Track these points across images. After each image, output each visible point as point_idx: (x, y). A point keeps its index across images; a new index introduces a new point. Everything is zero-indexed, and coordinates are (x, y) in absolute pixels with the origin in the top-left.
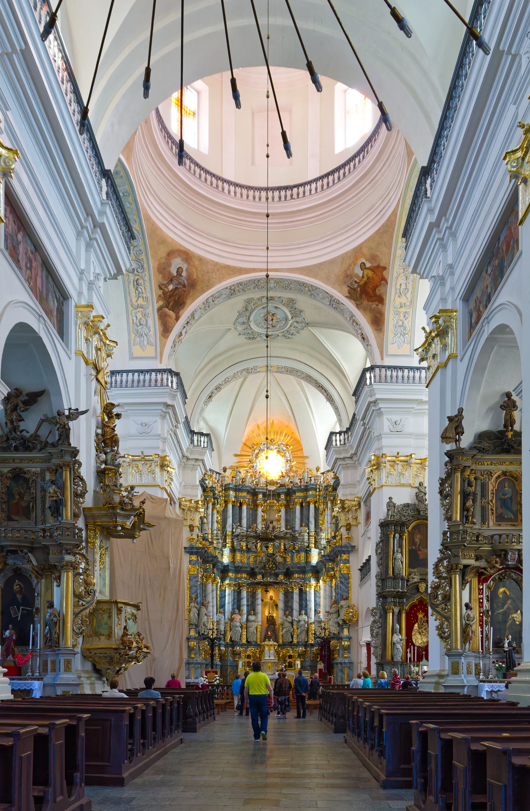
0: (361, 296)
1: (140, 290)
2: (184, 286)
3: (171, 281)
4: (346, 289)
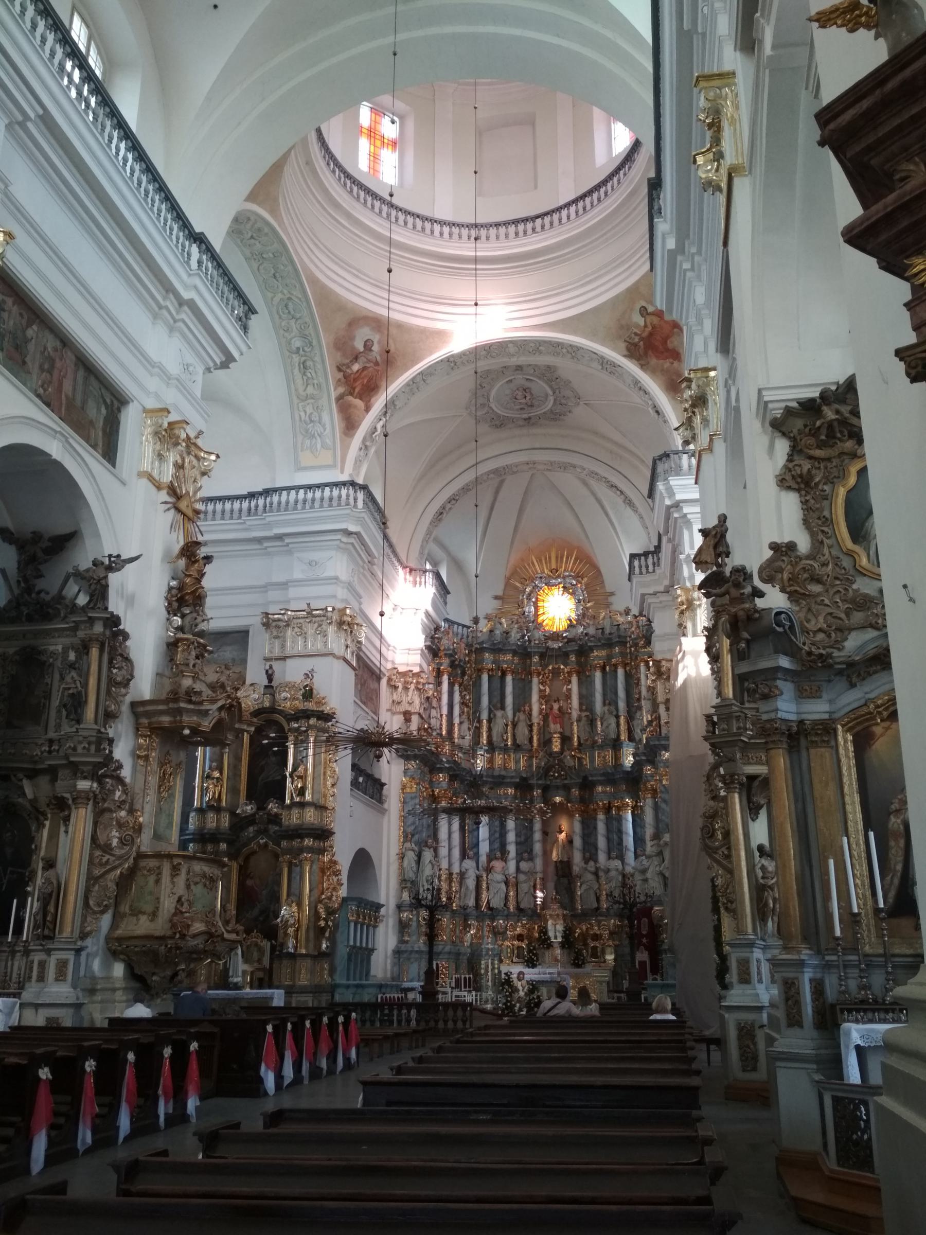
0: (646, 354)
1: (309, 375)
2: (377, 364)
3: (356, 358)
4: (623, 345)
